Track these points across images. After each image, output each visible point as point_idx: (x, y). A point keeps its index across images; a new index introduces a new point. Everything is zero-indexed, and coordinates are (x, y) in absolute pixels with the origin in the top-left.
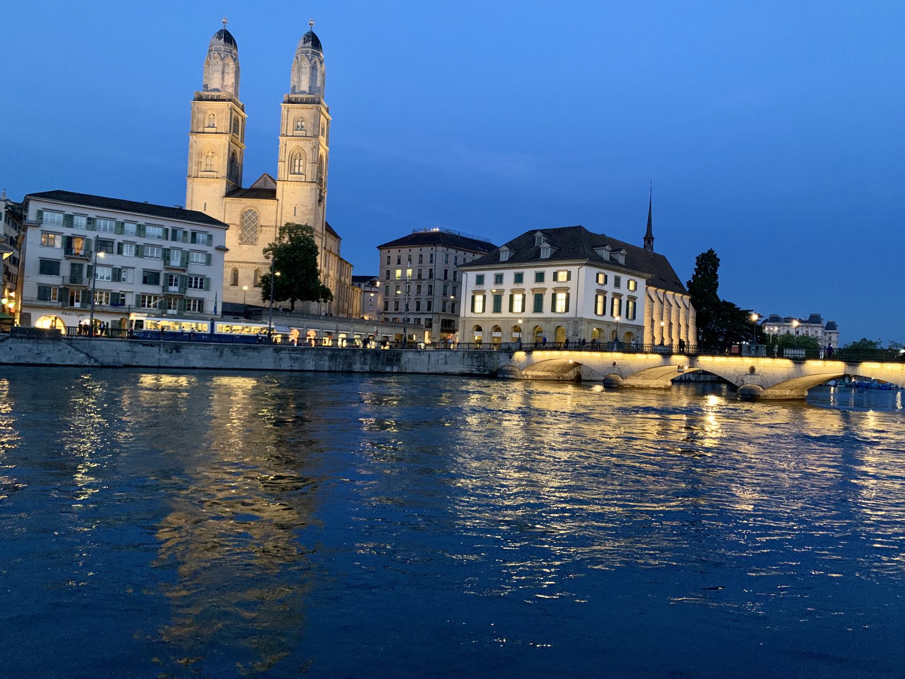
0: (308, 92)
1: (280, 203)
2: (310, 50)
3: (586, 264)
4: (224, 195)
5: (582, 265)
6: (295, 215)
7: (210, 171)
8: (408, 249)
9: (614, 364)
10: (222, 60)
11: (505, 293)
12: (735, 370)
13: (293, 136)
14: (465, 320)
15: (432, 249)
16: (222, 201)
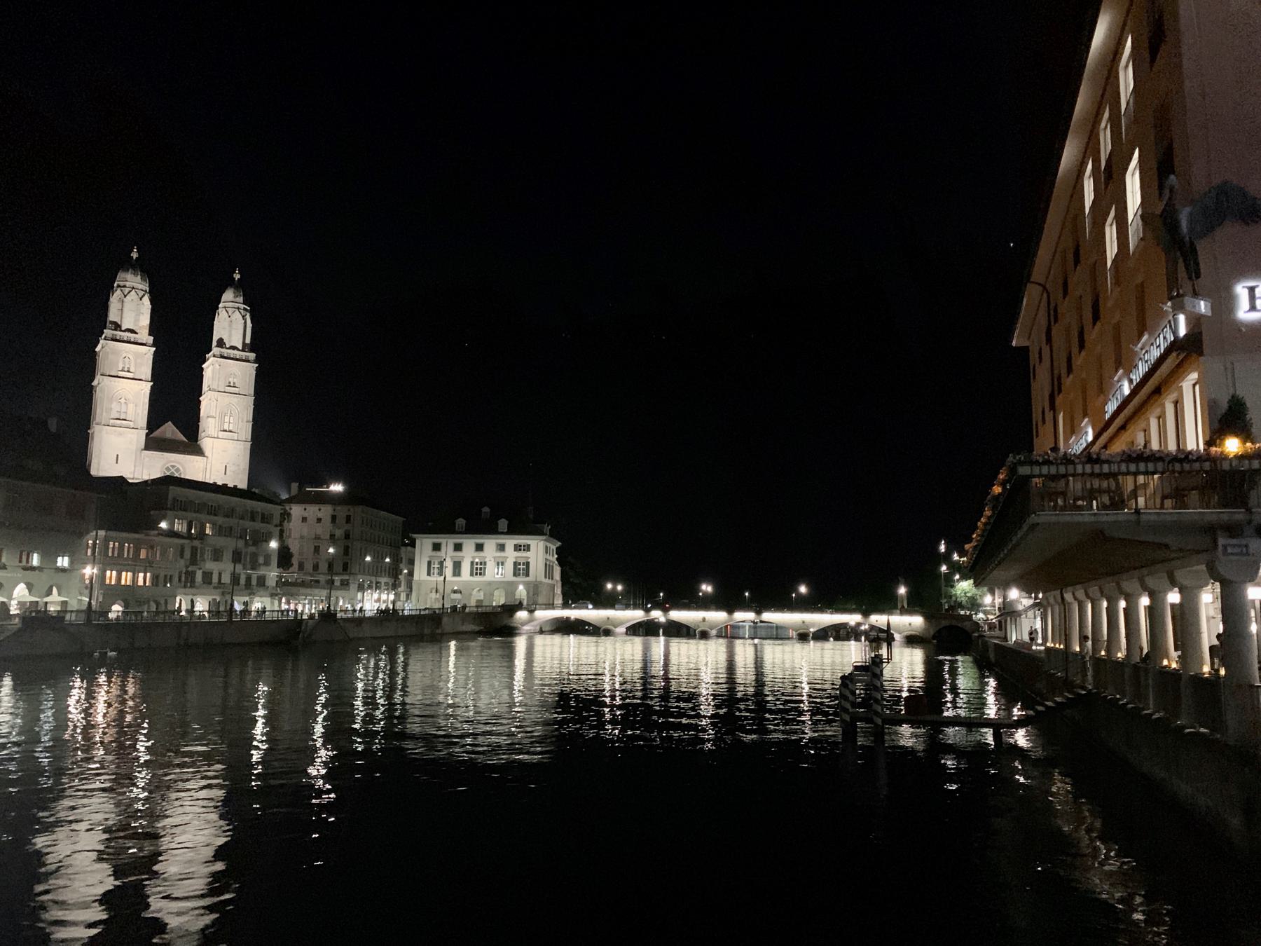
0: (240, 348)
1: (209, 461)
2: (242, 306)
3: (545, 540)
4: (143, 447)
5: (543, 540)
6: (225, 474)
7: (125, 420)
8: (317, 508)
9: (608, 618)
10: (141, 299)
11: (465, 559)
12: (694, 620)
13: (225, 392)
14: (420, 583)
15: (349, 510)
16: (141, 456)
